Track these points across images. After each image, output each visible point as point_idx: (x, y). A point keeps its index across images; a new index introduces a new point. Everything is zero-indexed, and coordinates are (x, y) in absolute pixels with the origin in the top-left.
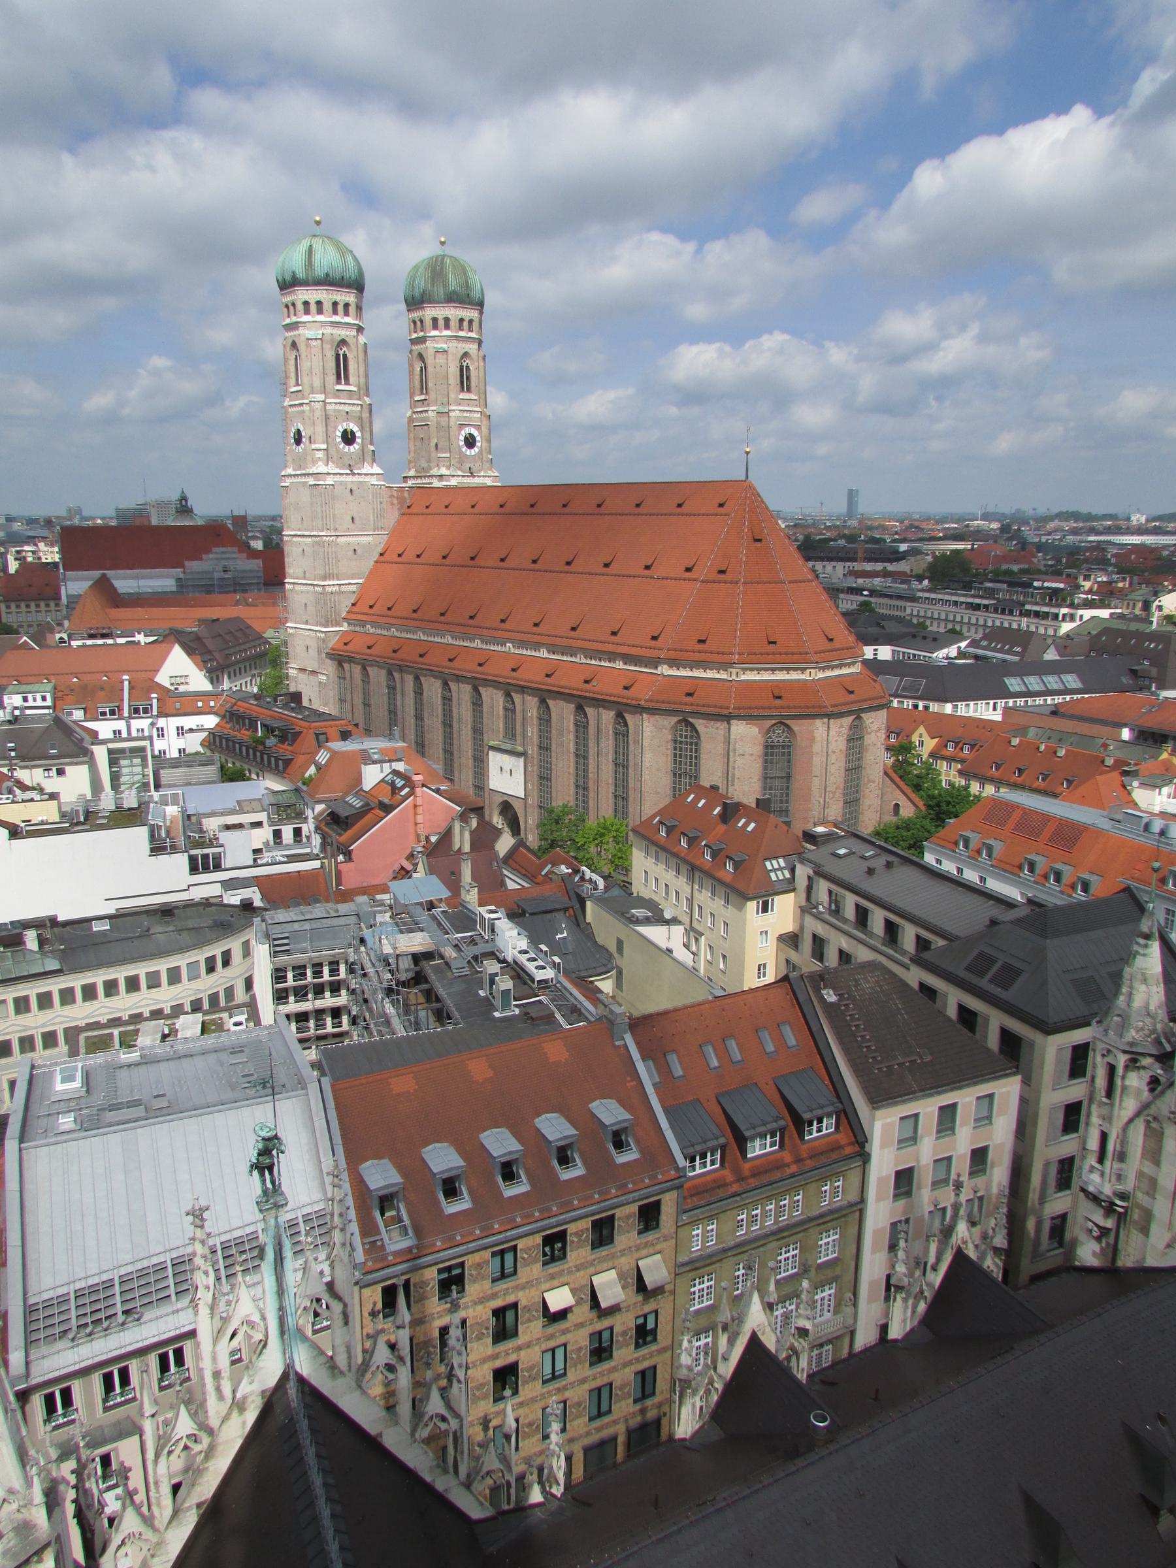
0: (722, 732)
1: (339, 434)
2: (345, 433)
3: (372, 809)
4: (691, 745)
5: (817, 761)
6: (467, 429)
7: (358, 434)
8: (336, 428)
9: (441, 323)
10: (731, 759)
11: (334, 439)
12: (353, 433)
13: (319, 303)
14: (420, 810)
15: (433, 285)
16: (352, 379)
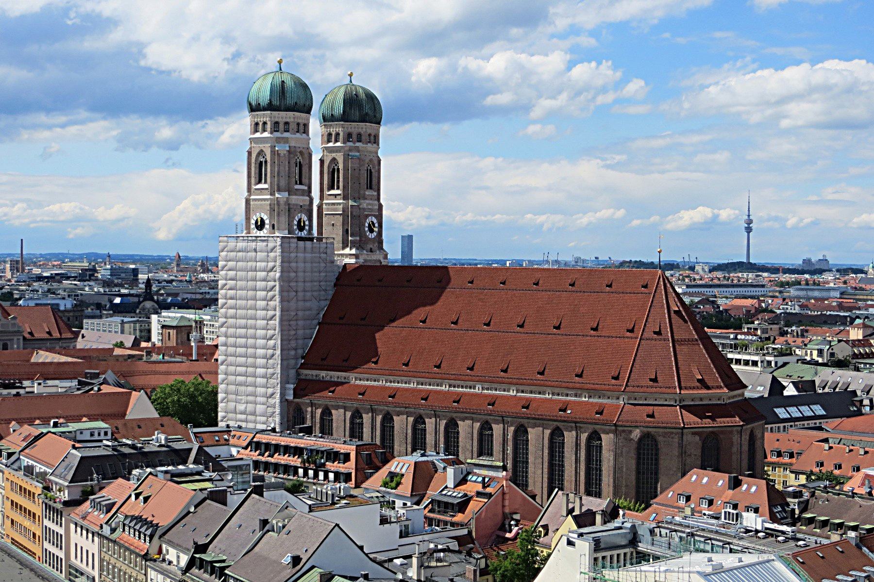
0: (677, 440)
1: (295, 223)
2: (299, 221)
3: (472, 497)
4: (652, 450)
5: (734, 457)
6: (370, 217)
7: (307, 223)
8: (294, 218)
9: (355, 137)
10: (684, 458)
11: (292, 226)
12: (304, 222)
13: (286, 123)
14: (507, 497)
15: (351, 109)
16: (304, 180)
